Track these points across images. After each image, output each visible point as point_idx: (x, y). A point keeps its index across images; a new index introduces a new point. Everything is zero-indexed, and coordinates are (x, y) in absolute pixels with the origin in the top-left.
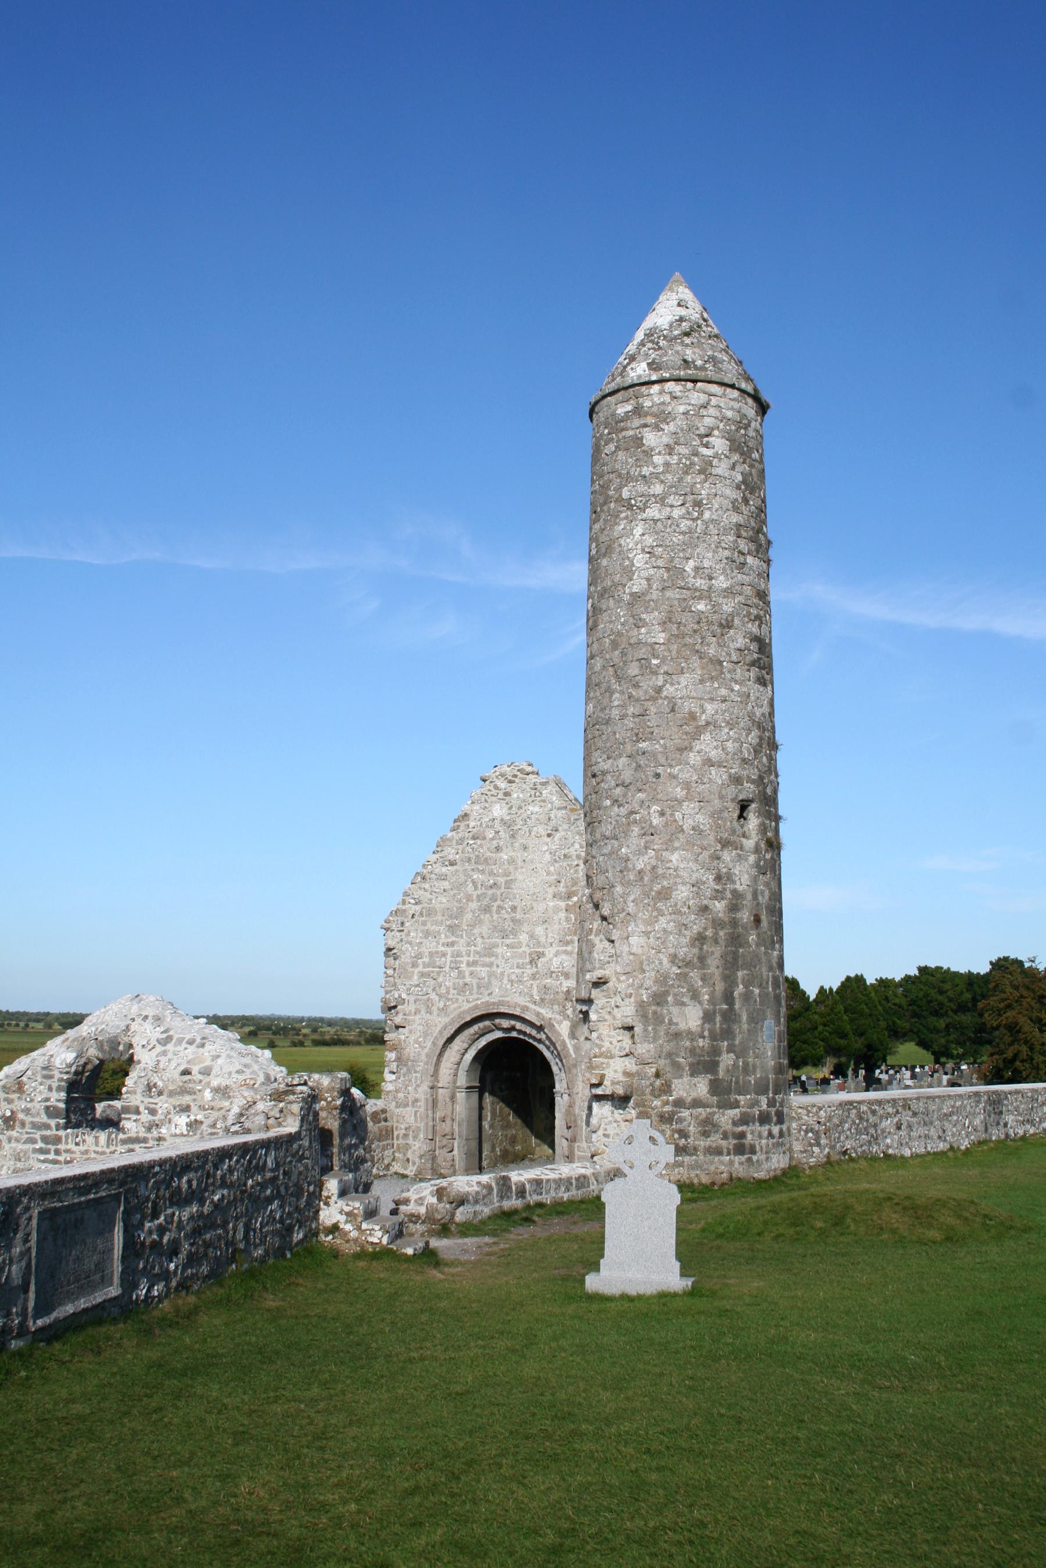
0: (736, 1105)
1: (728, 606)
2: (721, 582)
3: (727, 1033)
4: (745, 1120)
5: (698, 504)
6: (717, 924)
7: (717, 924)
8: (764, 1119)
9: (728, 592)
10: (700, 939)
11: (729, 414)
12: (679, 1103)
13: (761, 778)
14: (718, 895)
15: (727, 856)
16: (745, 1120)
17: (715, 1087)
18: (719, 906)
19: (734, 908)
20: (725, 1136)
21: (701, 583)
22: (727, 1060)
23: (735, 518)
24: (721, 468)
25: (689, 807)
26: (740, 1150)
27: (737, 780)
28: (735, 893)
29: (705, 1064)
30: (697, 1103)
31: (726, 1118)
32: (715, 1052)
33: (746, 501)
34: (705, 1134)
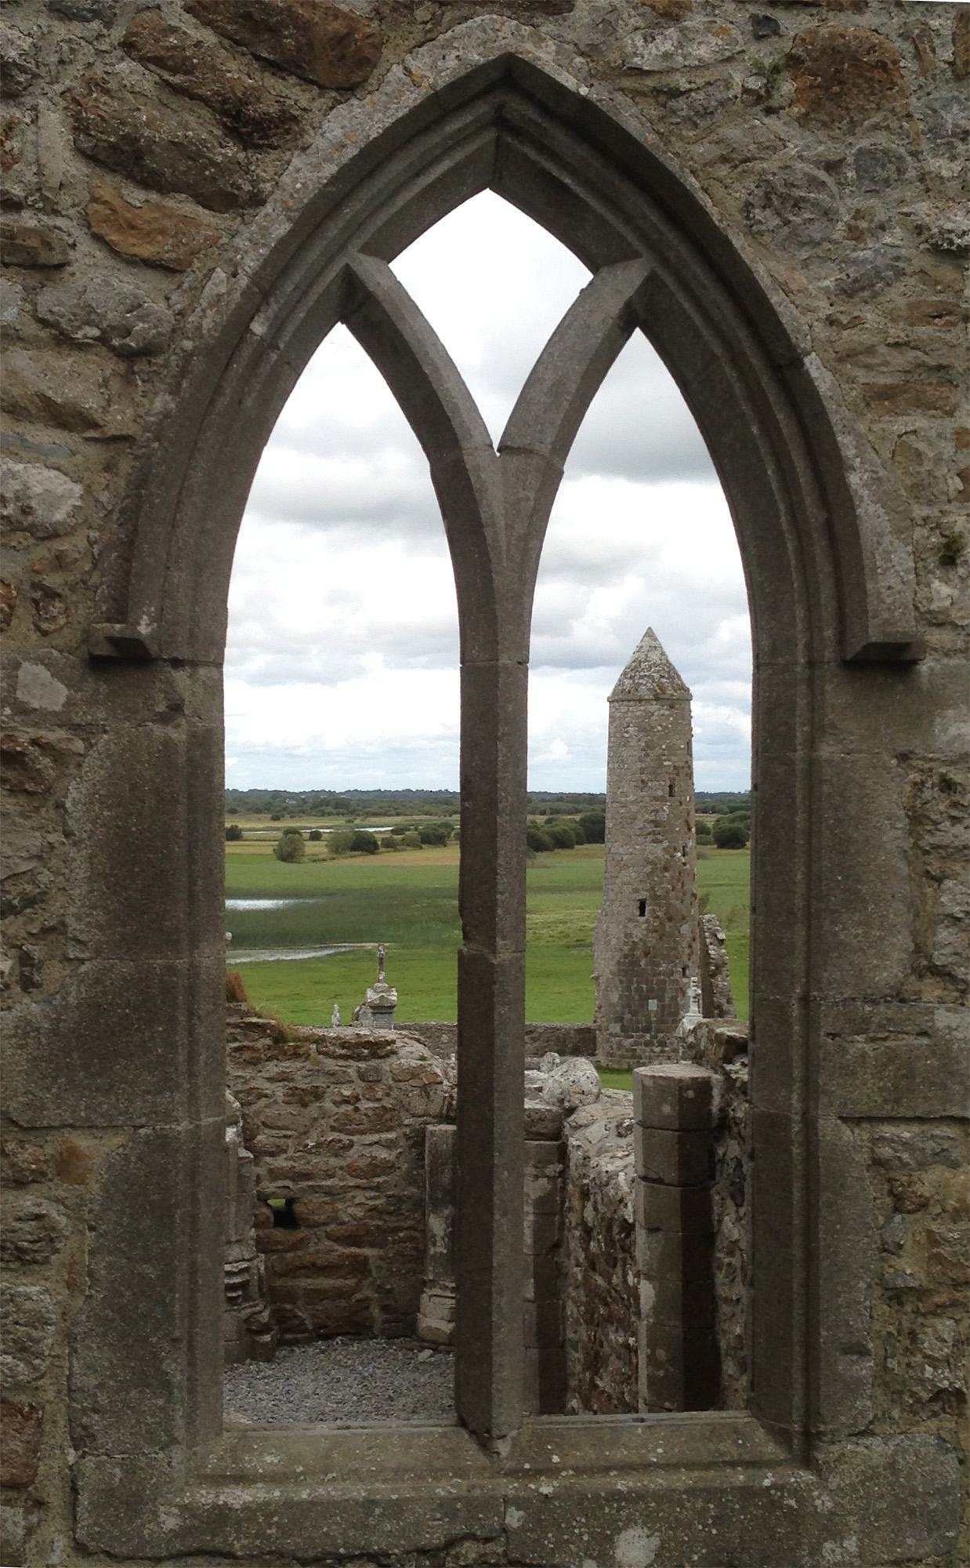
0: (632, 1037)
1: (634, 809)
2: (631, 798)
3: (629, 1006)
4: (636, 1044)
5: (623, 761)
6: (626, 957)
8: (647, 1044)
9: (634, 802)
10: (619, 963)
11: (639, 713)
12: (611, 1034)
13: (653, 888)
14: (626, 943)
15: (630, 925)
16: (636, 1044)
17: (623, 1029)
18: (626, 948)
19: (632, 949)
20: (627, 1051)
21: (623, 799)
22: (627, 1016)
23: (639, 765)
25: (617, 904)
26: (633, 1057)
27: (636, 891)
29: (619, 1019)
30: (616, 1035)
31: (628, 1042)
32: (623, 1013)
34: (619, 1049)
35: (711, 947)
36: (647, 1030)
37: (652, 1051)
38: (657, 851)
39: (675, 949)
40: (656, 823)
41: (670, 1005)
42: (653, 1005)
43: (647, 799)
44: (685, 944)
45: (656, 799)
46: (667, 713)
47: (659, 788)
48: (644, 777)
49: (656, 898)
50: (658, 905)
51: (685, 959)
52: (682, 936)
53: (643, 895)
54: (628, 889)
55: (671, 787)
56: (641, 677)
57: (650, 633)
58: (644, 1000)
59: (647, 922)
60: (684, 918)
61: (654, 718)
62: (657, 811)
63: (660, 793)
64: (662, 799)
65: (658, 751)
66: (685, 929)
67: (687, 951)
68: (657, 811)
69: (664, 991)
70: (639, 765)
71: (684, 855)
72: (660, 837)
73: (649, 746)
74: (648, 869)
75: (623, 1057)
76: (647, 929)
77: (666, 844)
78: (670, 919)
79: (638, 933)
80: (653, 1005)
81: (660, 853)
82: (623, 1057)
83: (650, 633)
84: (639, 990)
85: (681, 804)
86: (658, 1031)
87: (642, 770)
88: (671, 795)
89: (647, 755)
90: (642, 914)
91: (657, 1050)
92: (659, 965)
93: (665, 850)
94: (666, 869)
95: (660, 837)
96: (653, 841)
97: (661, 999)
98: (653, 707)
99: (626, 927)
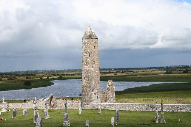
8: (85, 105)
9: (84, 58)
36: (85, 102)
42: (86, 97)
49: (87, 76)
50: (87, 78)
53: (85, 76)
58: (85, 96)
63: (87, 56)
64: (87, 58)
68: (87, 60)
70: (84, 51)
71: (93, 68)
74: (85, 71)
81: (87, 68)
86: (87, 102)
91: (87, 106)
93: (89, 67)
96: (86, 66)
98: (86, 40)
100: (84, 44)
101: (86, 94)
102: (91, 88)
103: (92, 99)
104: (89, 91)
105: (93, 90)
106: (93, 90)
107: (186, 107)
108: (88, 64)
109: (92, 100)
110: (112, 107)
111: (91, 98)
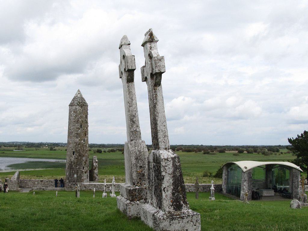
2: (72, 128)
3: (70, 176)
4: (71, 185)
7: (70, 165)
8: (74, 185)
9: (73, 129)
10: (68, 166)
14: (70, 161)
17: (69, 181)
19: (71, 163)
22: (70, 178)
24: (73, 115)
26: (71, 188)
27: (72, 149)
28: (72, 161)
29: (68, 179)
31: (70, 184)
33: (75, 118)
35: (94, 163)
36: (74, 182)
37: (75, 186)
38: (77, 140)
39: (81, 163)
40: (77, 134)
41: (79, 176)
42: (75, 176)
43: (75, 128)
44: (84, 162)
45: (77, 128)
46: (80, 108)
47: (78, 125)
48: (75, 123)
49: (77, 151)
51: (84, 165)
52: (83, 160)
53: (74, 150)
54: (71, 149)
55: (81, 125)
56: (75, 100)
57: (79, 91)
59: (75, 156)
60: (83, 156)
61: (77, 110)
62: (77, 131)
63: (78, 127)
65: (78, 117)
66: (84, 158)
67: (84, 164)
68: (77, 131)
69: (78, 172)
72: (78, 137)
73: (76, 116)
74: (75, 144)
75: (69, 188)
76: (75, 159)
77: (79, 139)
78: (80, 156)
79: (73, 159)
80: (75, 176)
81: (78, 141)
82: (69, 188)
83: (79, 91)
84: (72, 172)
85: (83, 129)
86: (76, 182)
87: (74, 122)
88: (81, 127)
89: (75, 118)
90: (74, 155)
92: (77, 167)
93: (79, 140)
94: (79, 144)
95: (78, 137)
96: (76, 138)
97: (77, 174)
98: (78, 107)
99: (70, 158)
100: (74, 112)
101: (75, 172)
102: (81, 165)
103: (82, 178)
104: (79, 168)
105: (83, 168)
106: (83, 168)
107: (190, 187)
108: (79, 136)
109: (83, 180)
110: (109, 187)
111: (81, 177)
